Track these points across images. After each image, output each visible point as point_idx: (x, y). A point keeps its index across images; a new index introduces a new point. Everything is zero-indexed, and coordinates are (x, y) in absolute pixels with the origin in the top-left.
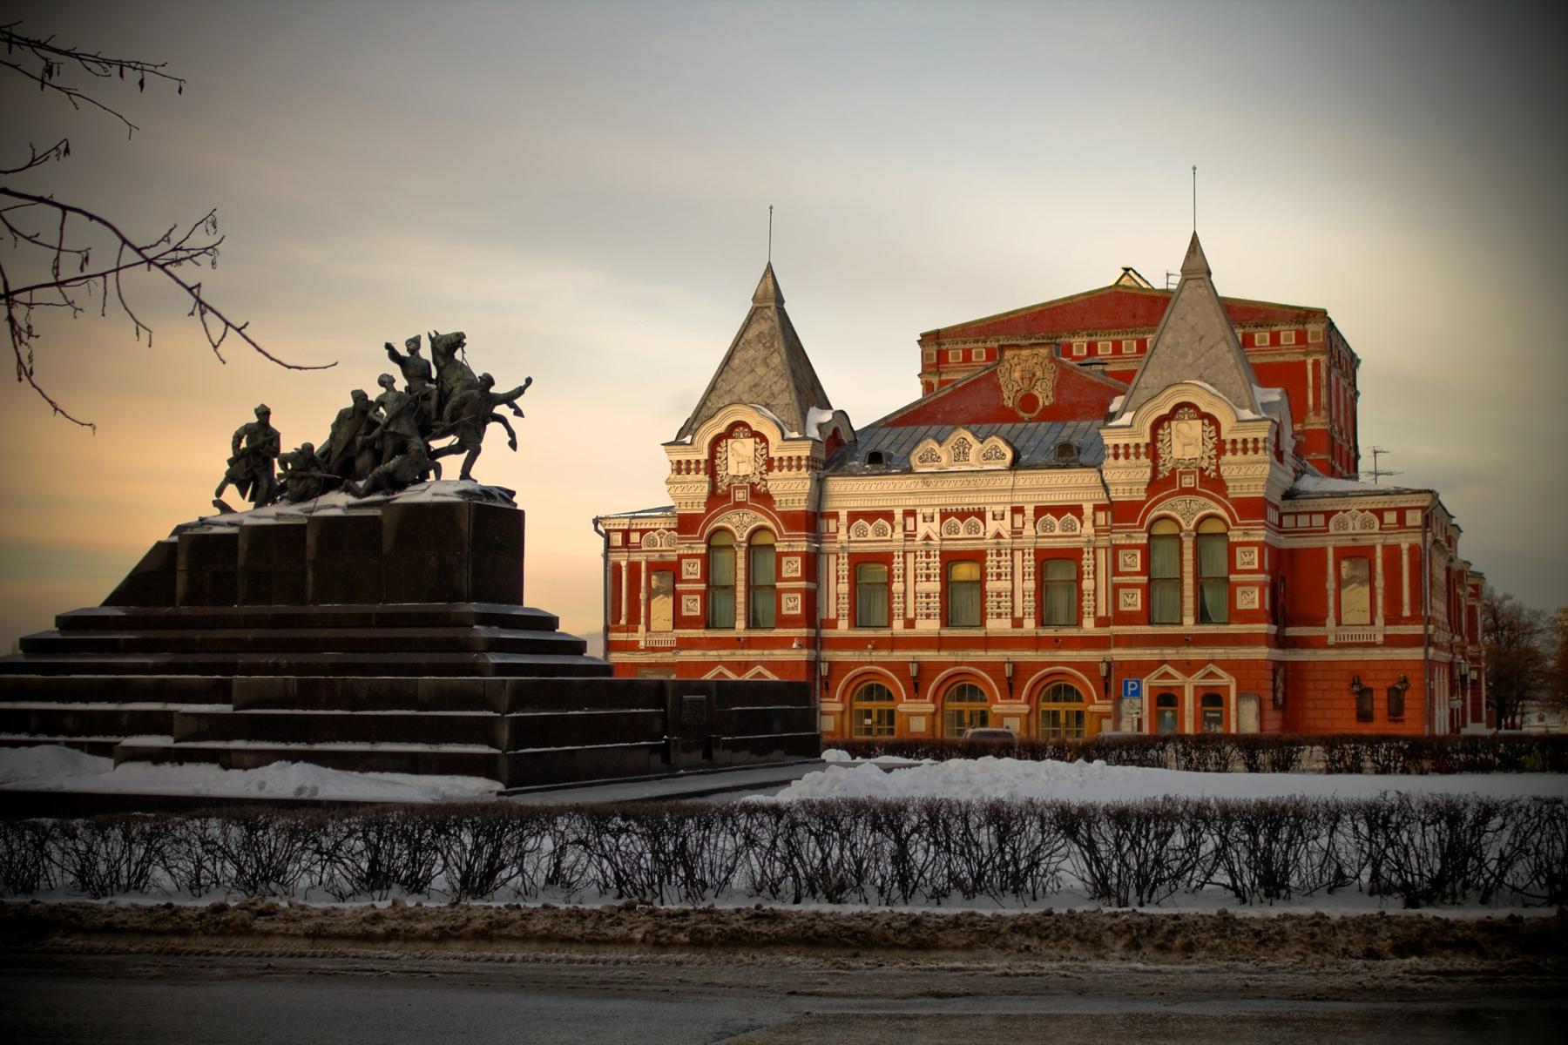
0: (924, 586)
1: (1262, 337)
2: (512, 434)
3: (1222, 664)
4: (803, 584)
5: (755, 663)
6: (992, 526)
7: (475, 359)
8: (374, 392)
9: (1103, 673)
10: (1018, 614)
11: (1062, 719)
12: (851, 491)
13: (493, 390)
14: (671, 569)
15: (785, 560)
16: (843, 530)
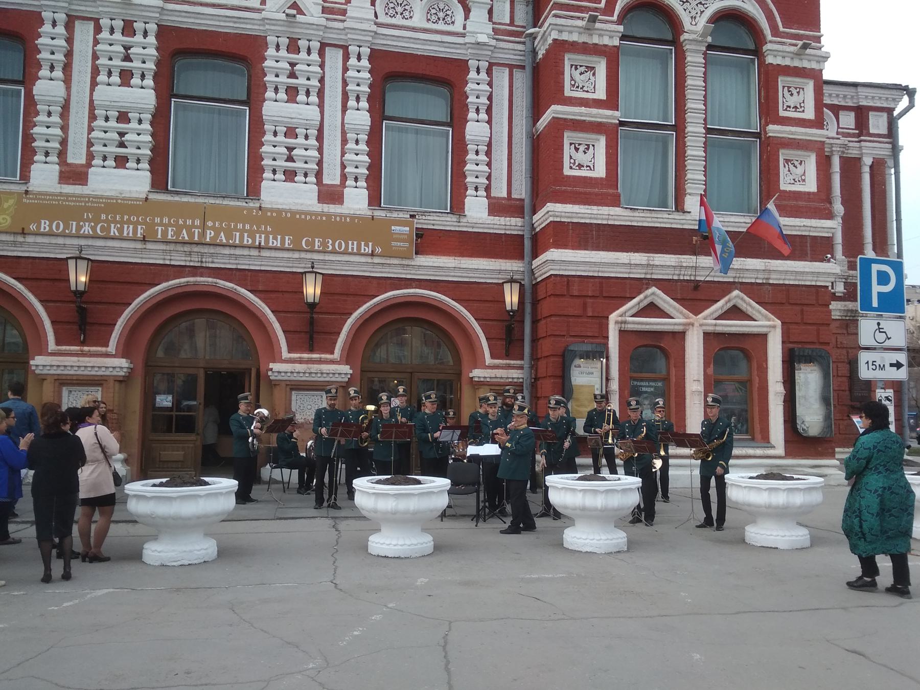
0: (111, 94)
10: (331, 177)
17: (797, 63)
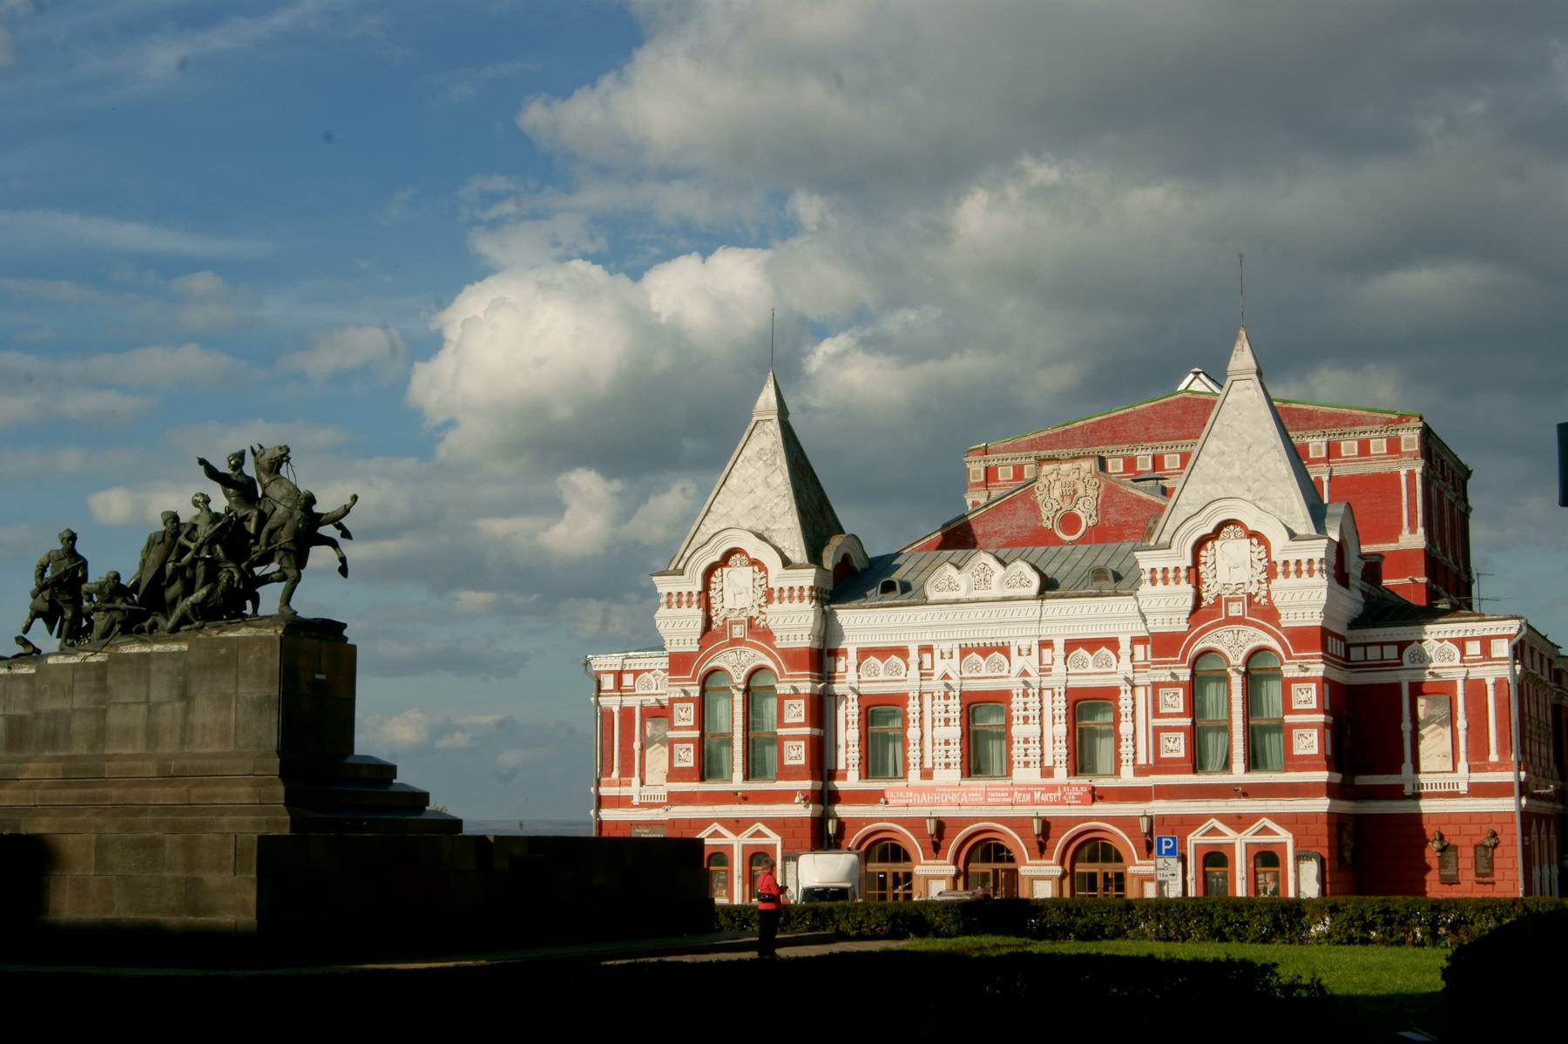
1: (1349, 447)
2: (343, 559)
3: (1278, 818)
4: (807, 731)
5: (752, 821)
6: (1018, 663)
7: (301, 475)
8: (187, 513)
9: (1144, 828)
10: (1048, 762)
11: (1100, 883)
12: (860, 624)
13: (317, 509)
14: (661, 713)
15: (787, 702)
16: (852, 668)
17: (1302, 675)
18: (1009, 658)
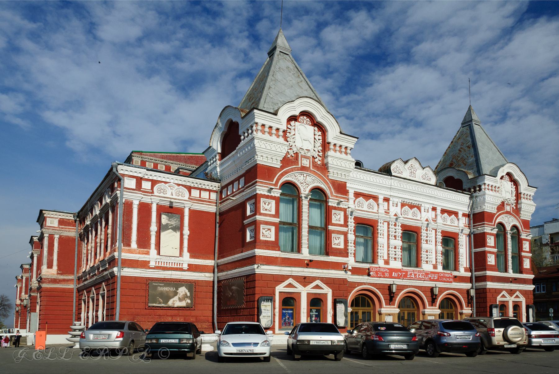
18: (420, 212)
